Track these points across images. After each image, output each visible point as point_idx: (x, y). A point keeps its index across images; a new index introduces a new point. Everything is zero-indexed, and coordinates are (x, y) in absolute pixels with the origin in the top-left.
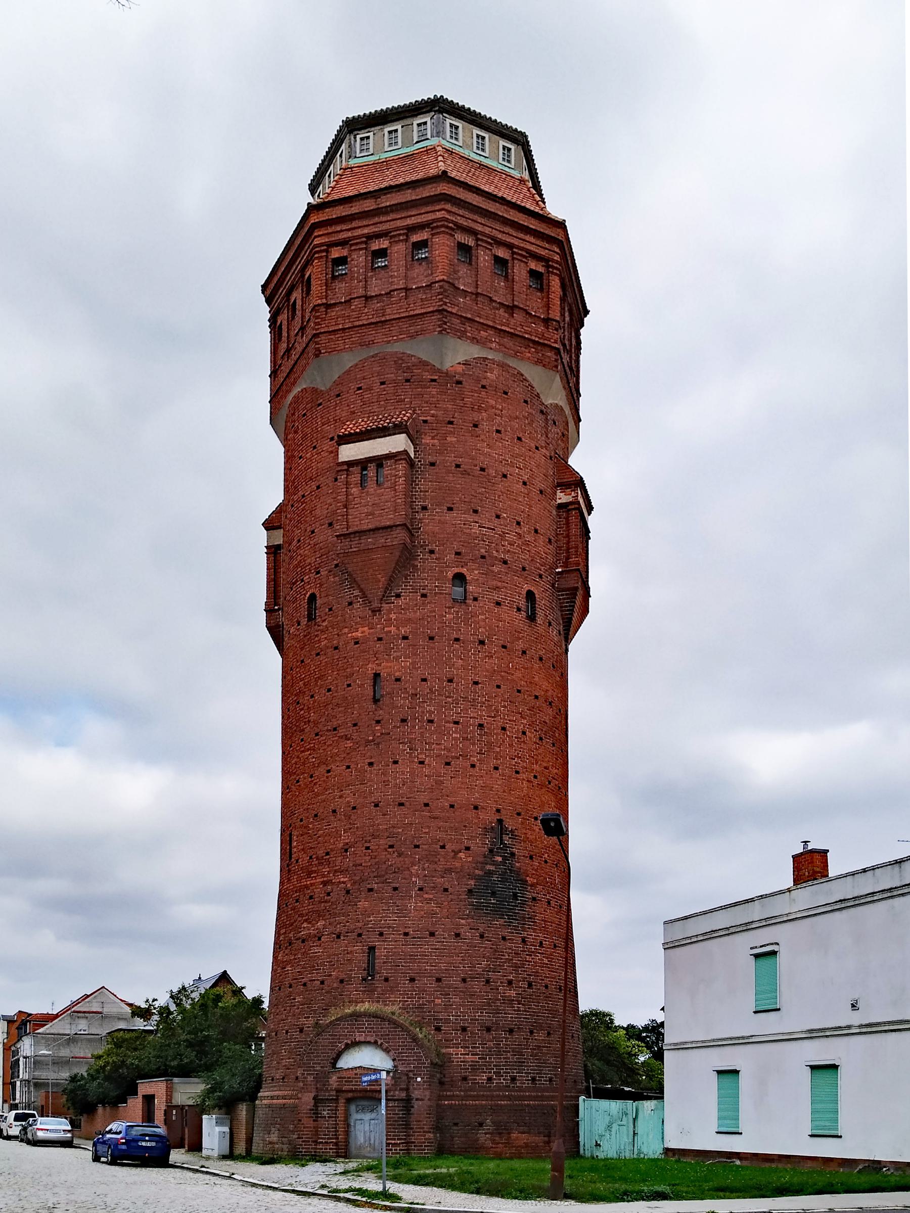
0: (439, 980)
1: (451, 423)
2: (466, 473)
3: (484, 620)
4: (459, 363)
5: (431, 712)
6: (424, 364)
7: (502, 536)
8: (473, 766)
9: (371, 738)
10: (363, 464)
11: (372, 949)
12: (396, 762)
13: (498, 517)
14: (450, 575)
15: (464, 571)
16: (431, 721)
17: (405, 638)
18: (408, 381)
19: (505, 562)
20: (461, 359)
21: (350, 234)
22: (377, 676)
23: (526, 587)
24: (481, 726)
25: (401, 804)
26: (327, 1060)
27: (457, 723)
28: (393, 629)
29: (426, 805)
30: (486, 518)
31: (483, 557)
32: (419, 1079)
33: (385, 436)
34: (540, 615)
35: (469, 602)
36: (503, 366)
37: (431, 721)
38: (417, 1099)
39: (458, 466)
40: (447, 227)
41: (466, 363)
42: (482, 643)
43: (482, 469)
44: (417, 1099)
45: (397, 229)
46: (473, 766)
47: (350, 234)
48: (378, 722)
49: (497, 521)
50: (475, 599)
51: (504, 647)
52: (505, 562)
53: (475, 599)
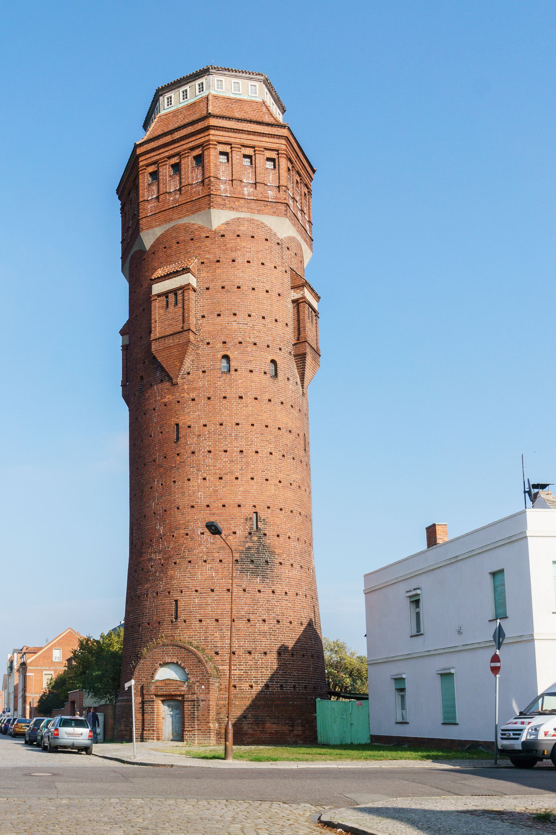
0: (217, 620)
1: (218, 261)
2: (228, 291)
3: (242, 383)
4: (223, 224)
5: (209, 446)
6: (201, 228)
7: (253, 327)
8: (237, 478)
9: (174, 465)
10: (166, 294)
11: (176, 601)
12: (189, 480)
13: (249, 316)
14: (219, 356)
15: (228, 353)
16: (210, 452)
17: (193, 400)
18: (192, 239)
19: (255, 344)
20: (224, 221)
21: (158, 157)
22: (177, 425)
23: (270, 358)
24: (241, 451)
25: (193, 507)
26: (149, 675)
27: (226, 451)
28: (186, 395)
29: (208, 506)
30: (242, 317)
31: (240, 343)
32: (203, 687)
33: (178, 276)
34: (280, 373)
35: (232, 372)
36: (251, 221)
37: (210, 452)
38: (202, 700)
39: (223, 288)
40: (212, 144)
41: (227, 223)
42: (241, 397)
43: (239, 287)
44: (202, 700)
45: (184, 150)
46: (237, 478)
47: (158, 157)
48: (178, 455)
49: (249, 318)
50: (236, 370)
51: (256, 399)
52: (255, 344)
53: (236, 370)
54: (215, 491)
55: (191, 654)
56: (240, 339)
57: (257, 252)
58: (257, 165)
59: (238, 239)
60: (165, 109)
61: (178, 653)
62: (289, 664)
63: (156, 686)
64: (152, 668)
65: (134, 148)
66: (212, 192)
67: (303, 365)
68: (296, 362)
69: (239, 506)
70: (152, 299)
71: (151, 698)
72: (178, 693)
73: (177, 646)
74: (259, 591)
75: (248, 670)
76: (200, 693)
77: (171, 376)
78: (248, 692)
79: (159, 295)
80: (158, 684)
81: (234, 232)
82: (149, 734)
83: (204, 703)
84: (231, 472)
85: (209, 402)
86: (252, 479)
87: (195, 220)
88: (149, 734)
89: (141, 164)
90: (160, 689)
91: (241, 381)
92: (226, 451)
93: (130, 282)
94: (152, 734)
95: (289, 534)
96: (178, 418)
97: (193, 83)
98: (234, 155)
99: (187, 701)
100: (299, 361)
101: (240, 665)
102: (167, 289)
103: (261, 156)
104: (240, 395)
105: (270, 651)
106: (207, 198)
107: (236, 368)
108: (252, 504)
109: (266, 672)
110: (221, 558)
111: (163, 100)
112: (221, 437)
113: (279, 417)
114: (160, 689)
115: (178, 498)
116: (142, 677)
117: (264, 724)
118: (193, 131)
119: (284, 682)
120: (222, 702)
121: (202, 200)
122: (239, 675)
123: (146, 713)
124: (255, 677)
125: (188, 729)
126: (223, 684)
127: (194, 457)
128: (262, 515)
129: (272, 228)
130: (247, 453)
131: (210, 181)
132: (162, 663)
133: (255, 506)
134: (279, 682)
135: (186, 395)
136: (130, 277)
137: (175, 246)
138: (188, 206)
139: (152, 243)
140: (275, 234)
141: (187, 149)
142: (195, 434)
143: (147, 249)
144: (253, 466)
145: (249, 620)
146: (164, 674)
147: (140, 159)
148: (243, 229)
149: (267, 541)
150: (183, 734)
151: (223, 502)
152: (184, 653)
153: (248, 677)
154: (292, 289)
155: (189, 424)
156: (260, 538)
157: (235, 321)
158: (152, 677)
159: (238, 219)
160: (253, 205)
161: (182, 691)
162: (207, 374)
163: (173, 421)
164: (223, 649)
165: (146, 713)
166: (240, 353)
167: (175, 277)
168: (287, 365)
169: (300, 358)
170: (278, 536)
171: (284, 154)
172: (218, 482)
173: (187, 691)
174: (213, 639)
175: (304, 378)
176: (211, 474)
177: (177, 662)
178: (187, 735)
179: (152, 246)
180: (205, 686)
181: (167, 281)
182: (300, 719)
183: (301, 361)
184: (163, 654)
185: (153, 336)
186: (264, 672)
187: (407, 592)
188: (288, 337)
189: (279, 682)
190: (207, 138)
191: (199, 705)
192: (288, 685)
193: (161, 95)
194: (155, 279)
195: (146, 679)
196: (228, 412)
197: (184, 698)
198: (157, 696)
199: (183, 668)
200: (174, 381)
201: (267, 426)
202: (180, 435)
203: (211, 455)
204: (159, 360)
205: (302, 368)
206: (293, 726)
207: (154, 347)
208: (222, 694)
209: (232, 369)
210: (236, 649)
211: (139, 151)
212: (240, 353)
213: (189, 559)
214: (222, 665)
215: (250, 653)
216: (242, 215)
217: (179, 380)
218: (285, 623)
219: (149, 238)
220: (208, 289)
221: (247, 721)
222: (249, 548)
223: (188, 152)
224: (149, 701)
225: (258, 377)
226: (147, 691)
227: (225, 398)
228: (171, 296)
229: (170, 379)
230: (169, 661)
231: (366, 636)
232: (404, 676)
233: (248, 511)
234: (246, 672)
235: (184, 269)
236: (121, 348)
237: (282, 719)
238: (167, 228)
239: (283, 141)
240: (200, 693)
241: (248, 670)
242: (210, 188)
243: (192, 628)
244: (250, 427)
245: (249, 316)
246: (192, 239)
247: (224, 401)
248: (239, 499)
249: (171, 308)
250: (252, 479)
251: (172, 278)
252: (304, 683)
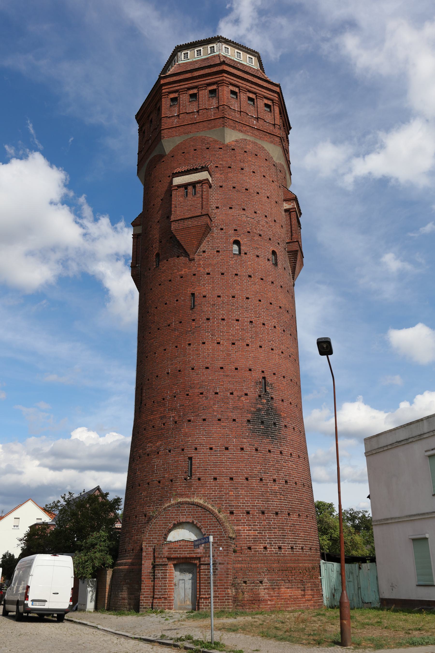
0: (231, 479)
1: (230, 167)
2: (238, 191)
3: (251, 265)
4: (233, 141)
5: (223, 314)
6: (216, 141)
7: (258, 222)
8: (248, 345)
9: (189, 329)
10: (185, 186)
11: (190, 458)
12: (204, 343)
13: (255, 213)
14: (232, 240)
15: (239, 239)
16: (223, 319)
17: (208, 274)
18: (208, 148)
19: (260, 235)
20: (234, 139)
21: (179, 88)
22: (193, 294)
23: (272, 248)
24: (251, 322)
25: (207, 368)
26: (161, 536)
27: (238, 320)
28: (202, 269)
29: (222, 368)
30: (249, 212)
31: (249, 232)
32: (221, 549)
33: (197, 172)
34: (279, 263)
35: (243, 255)
36: (254, 143)
37: (223, 319)
38: (220, 564)
39: (234, 188)
40: (226, 83)
41: (236, 141)
42: (250, 276)
43: (247, 190)
44: (220, 564)
45: (202, 85)
46: (248, 345)
47: (179, 88)
48: (194, 320)
49: (255, 215)
50: (246, 254)
51: (262, 279)
52: (260, 235)
53: (246, 254)
54: (229, 355)
55: (208, 513)
56: (249, 229)
57: (260, 167)
58: (259, 106)
59: (245, 154)
60: (182, 59)
61: (194, 512)
62: (297, 525)
63: (169, 548)
64: (166, 528)
65: (158, 79)
66: (225, 116)
67: (294, 260)
68: (289, 257)
69: (250, 370)
70: (173, 188)
71: (163, 562)
72: (194, 555)
73: (193, 504)
74: (269, 451)
75: (263, 530)
76: (218, 556)
77: (189, 252)
78: (262, 554)
79: (179, 186)
80: (172, 546)
81: (242, 148)
82: (159, 603)
83: (222, 566)
84: (243, 339)
85: (222, 277)
86: (261, 347)
87: (211, 135)
88: (159, 603)
89: (164, 91)
90: (173, 551)
91: (250, 263)
92: (238, 320)
93: (145, 185)
94: (162, 603)
95: (290, 400)
96: (194, 288)
97: (206, 46)
98: (242, 95)
99: (158, 565)
100: (291, 256)
101: (255, 525)
102: (187, 182)
103: (261, 101)
104: (250, 274)
105: (281, 512)
106: (221, 119)
107: (246, 251)
108: (261, 369)
109: (279, 533)
110: (234, 417)
111: (181, 55)
112: (234, 307)
113: (280, 297)
114: (173, 551)
115: (193, 359)
116: (153, 538)
117: (279, 589)
118: (209, 72)
119: (294, 544)
120: (239, 565)
121: (217, 121)
122: (254, 535)
123: (157, 578)
124: (269, 538)
125: (204, 596)
126: (238, 546)
127: (210, 323)
128: (269, 380)
129: (270, 152)
130: (255, 324)
131: (224, 107)
132: (176, 523)
133: (263, 372)
134: (290, 544)
135: (202, 269)
136: (145, 180)
137: (193, 152)
138: (205, 124)
139: (171, 149)
140: (272, 158)
141: (205, 84)
142: (210, 304)
143: (167, 153)
144: (261, 336)
145: (261, 480)
146: (176, 535)
147: (163, 88)
148: (249, 147)
149: (277, 404)
150: (199, 603)
151: (236, 365)
152: (200, 512)
153: (262, 538)
154: (284, 201)
155: (204, 294)
156: (268, 401)
157: (245, 215)
158: (165, 538)
159: (245, 140)
160: (256, 132)
161: (198, 553)
162: (220, 253)
163: (190, 291)
164: (238, 508)
165: (157, 578)
166: (249, 241)
167: (194, 173)
168: (284, 259)
169: (292, 254)
170: (282, 400)
171: (277, 103)
172: (231, 347)
173: (204, 553)
174: (228, 498)
175: (295, 271)
176: (224, 340)
177: (193, 522)
178: (203, 603)
179: (172, 151)
180: (223, 548)
181: (187, 176)
182: (310, 582)
183: (293, 256)
184: (177, 513)
185: (173, 218)
186: (276, 533)
187: (426, 451)
188: (283, 236)
189: (290, 544)
190: (221, 78)
191: (217, 569)
192: (297, 546)
193: (179, 51)
194: (176, 173)
195: (158, 541)
196: (239, 287)
197: (200, 561)
198: (169, 559)
199: (199, 529)
200: (191, 257)
201: (271, 304)
202: (196, 304)
203: (224, 323)
204: (178, 238)
205: (293, 263)
206: (304, 590)
207: (173, 226)
208: (238, 557)
209: (243, 252)
210: (251, 508)
211: (162, 82)
212: (249, 241)
213: (204, 417)
214: (237, 525)
215: (263, 513)
216: (248, 138)
217: (196, 257)
218: (291, 483)
219: (169, 144)
220: (221, 187)
221: (263, 586)
222: (259, 410)
223: (205, 87)
224: (161, 565)
225: (262, 261)
226: (159, 554)
227: (236, 275)
228: (190, 188)
229: (187, 255)
230: (184, 521)
231: (369, 497)
232: (427, 536)
233: (258, 376)
234: (260, 533)
235: (202, 167)
236: (132, 236)
237: (295, 583)
238: (186, 138)
239: (276, 95)
240: (218, 556)
241: (263, 530)
242: (223, 113)
243: (207, 486)
244: (258, 302)
245: (255, 213)
246: (208, 148)
247: (236, 278)
248: (250, 364)
249: (190, 197)
250: (261, 347)
251: (192, 173)
252: (309, 545)
